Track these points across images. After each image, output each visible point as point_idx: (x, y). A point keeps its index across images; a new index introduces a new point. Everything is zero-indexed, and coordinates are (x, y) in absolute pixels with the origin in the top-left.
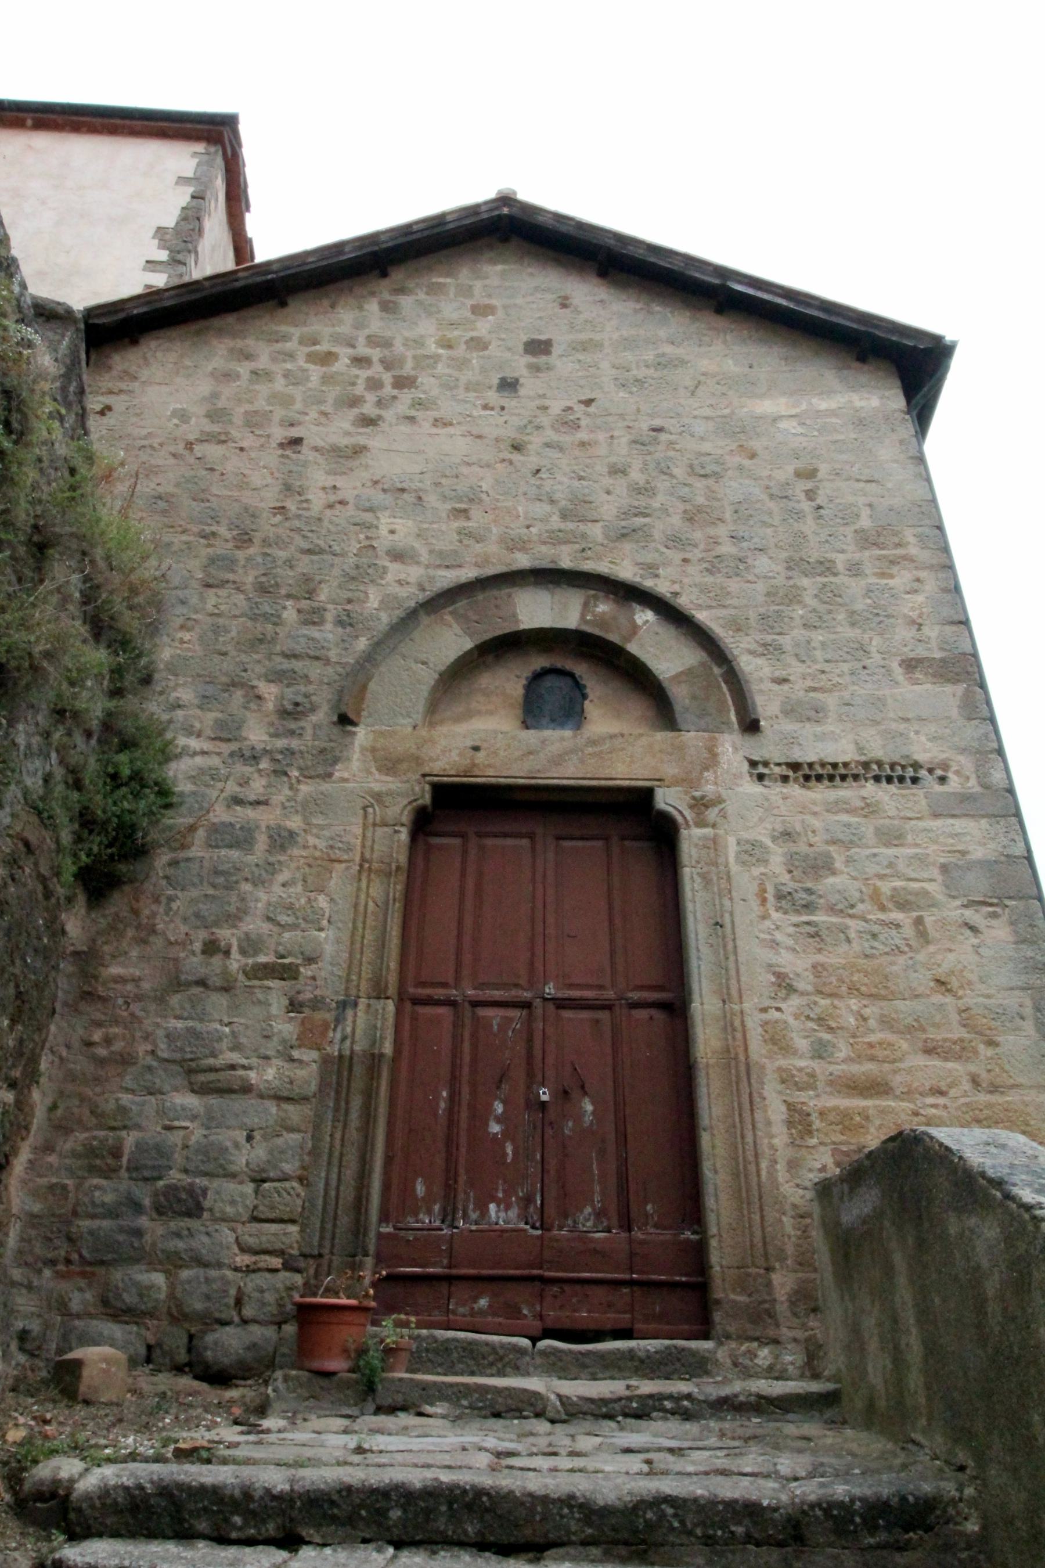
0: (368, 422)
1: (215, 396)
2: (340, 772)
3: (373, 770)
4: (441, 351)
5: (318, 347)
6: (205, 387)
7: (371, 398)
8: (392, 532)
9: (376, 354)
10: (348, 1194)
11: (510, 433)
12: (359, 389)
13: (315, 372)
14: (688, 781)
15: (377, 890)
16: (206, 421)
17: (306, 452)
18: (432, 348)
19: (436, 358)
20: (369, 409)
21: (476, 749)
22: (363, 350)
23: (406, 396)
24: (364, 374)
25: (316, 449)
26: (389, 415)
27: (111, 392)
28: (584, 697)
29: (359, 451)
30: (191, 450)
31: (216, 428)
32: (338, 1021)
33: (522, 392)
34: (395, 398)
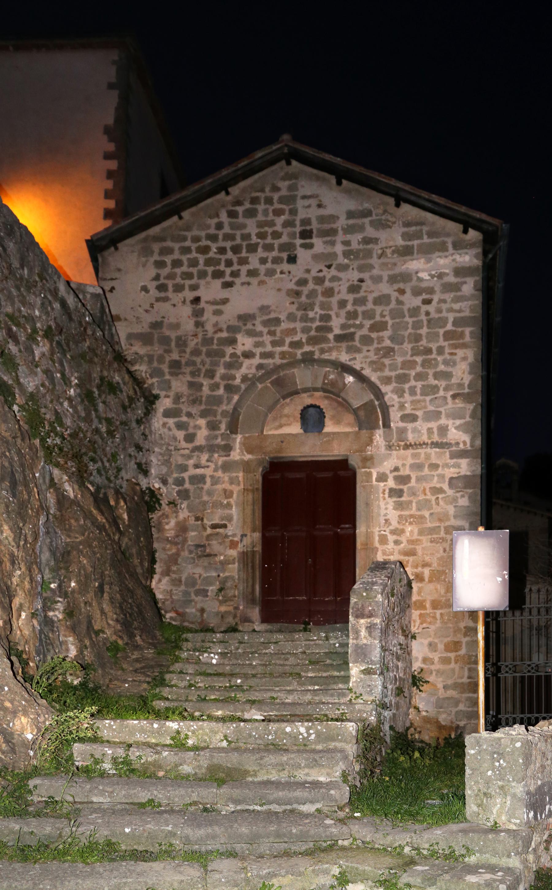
0: (228, 285)
1: (157, 278)
2: (232, 453)
3: (245, 453)
4: (259, 240)
5: (200, 243)
6: (153, 272)
7: (228, 271)
8: (243, 345)
9: (228, 245)
10: (250, 590)
11: (292, 286)
12: (222, 267)
13: (201, 259)
14: (362, 450)
15: (250, 497)
16: (157, 291)
17: (202, 304)
18: (254, 239)
19: (257, 244)
20: (228, 278)
21: (282, 442)
22: (221, 244)
23: (244, 269)
24: (223, 257)
25: (207, 302)
26: (238, 281)
27: (112, 279)
28: (325, 417)
29: (225, 301)
30: (153, 307)
31: (163, 295)
32: (241, 541)
33: (299, 261)
34: (239, 270)
